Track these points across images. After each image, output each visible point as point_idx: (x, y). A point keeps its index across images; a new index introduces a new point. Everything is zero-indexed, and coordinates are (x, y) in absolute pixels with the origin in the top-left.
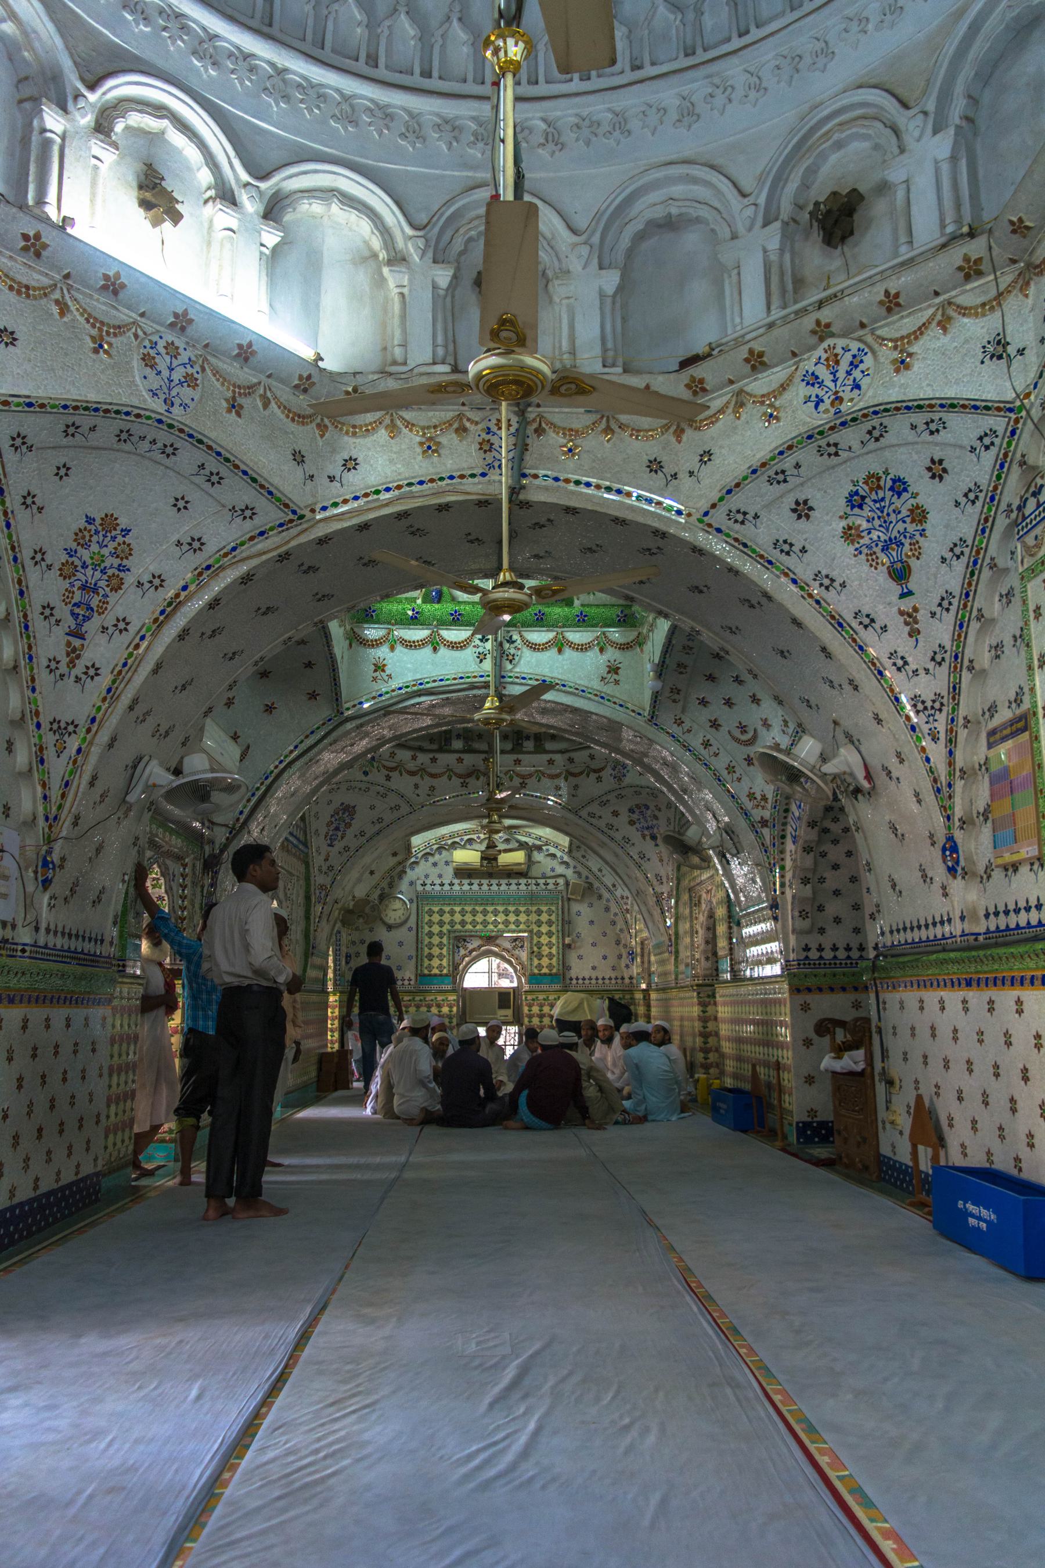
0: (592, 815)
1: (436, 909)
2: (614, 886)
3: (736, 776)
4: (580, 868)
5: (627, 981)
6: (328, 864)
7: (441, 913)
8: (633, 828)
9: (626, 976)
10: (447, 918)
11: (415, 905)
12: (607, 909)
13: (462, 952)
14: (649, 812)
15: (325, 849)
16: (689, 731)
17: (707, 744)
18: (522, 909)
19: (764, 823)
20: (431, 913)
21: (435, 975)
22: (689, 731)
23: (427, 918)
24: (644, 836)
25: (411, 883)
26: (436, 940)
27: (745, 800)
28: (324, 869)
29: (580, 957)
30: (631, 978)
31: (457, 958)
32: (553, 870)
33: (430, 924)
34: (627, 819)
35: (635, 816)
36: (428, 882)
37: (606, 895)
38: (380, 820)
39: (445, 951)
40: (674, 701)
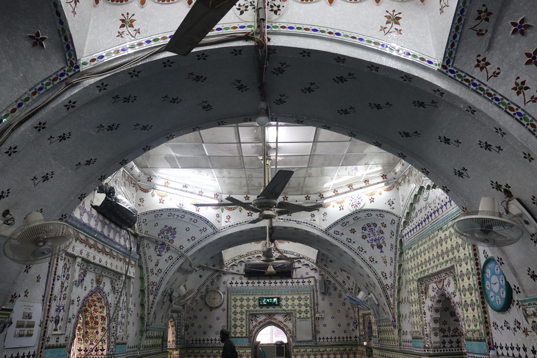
0: (337, 233)
1: (238, 298)
2: (344, 282)
4: (323, 273)
5: (353, 339)
6: (158, 268)
7: (242, 300)
8: (366, 241)
9: (353, 336)
10: (245, 303)
11: (226, 295)
12: (340, 296)
13: (254, 323)
14: (377, 229)
15: (155, 258)
18: (290, 297)
20: (235, 300)
21: (238, 337)
23: (233, 303)
24: (372, 246)
25: (224, 283)
26: (239, 316)
28: (155, 271)
29: (325, 325)
30: (356, 337)
31: (251, 327)
32: (307, 274)
33: (235, 306)
34: (361, 235)
35: (366, 233)
36: (234, 282)
37: (339, 288)
38: (193, 238)
39: (244, 323)
40: (480, 33)
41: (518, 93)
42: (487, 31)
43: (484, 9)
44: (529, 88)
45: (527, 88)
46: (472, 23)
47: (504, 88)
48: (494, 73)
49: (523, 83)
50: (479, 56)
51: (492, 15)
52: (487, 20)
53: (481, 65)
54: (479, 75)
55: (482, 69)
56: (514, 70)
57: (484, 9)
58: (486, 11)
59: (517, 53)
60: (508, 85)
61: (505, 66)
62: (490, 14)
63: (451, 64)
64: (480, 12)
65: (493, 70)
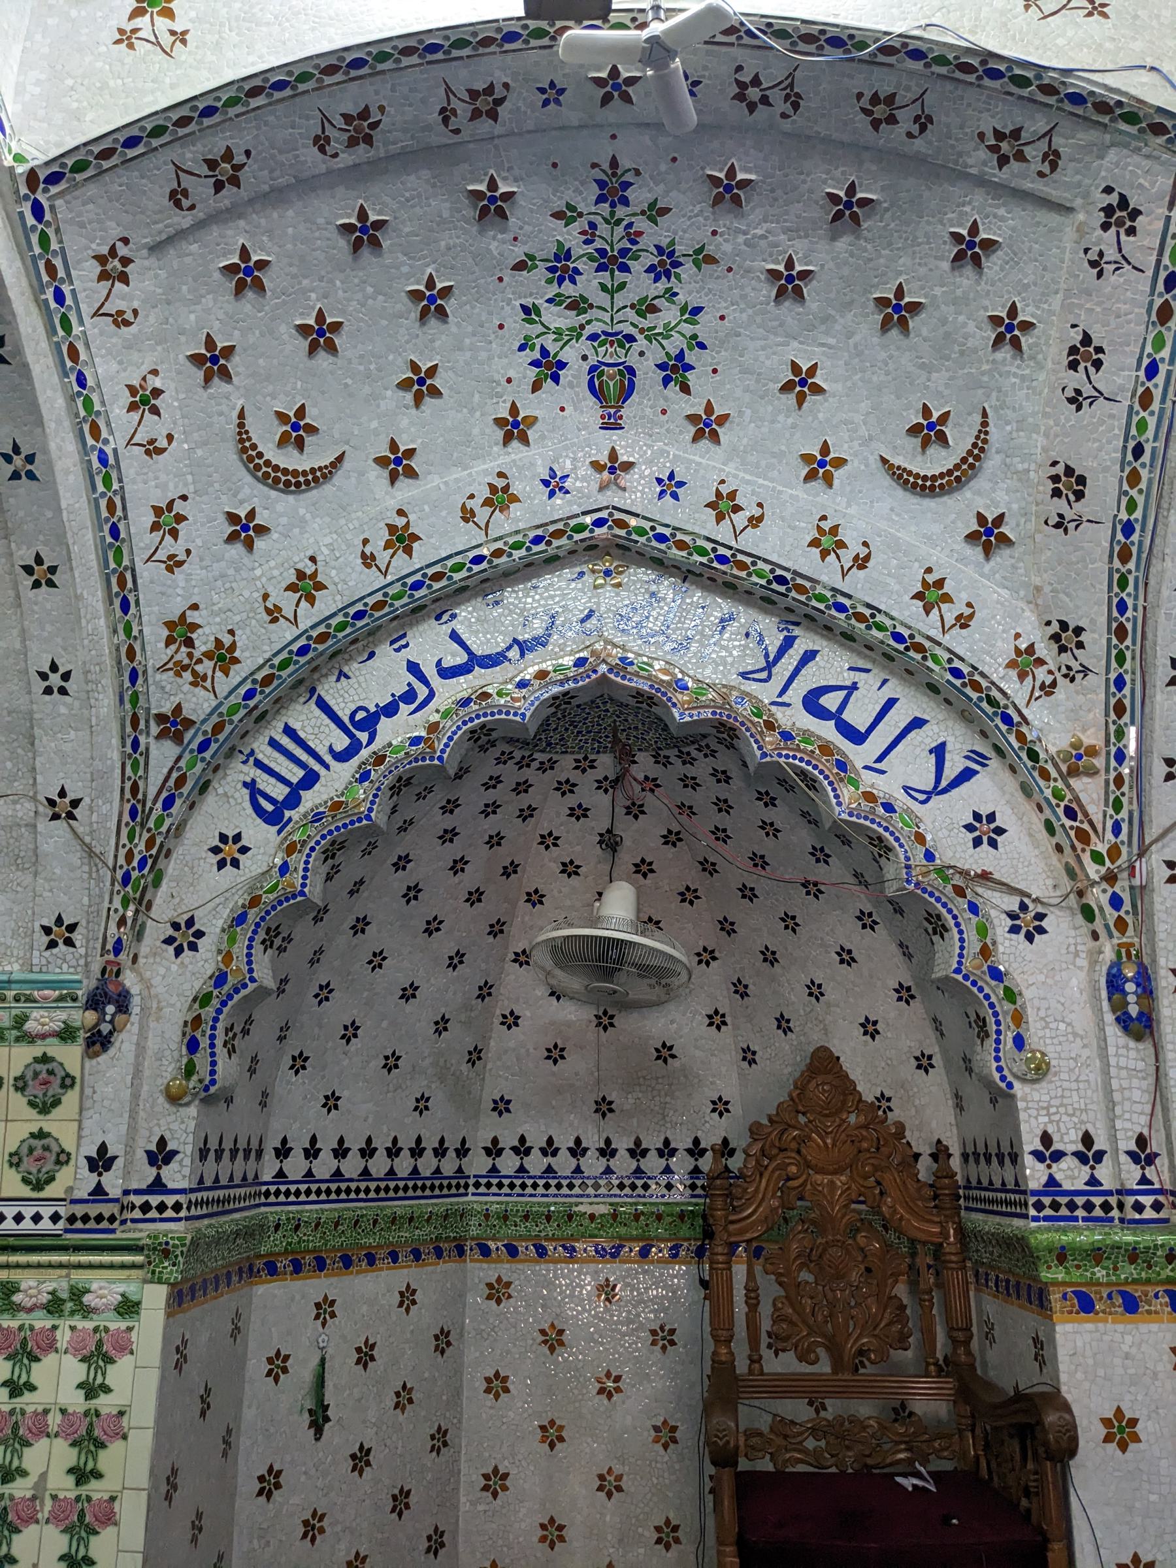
3: (170, 546)
16: (120, 320)
17: (144, 400)
19: (174, 725)
22: (120, 320)
27: (154, 634)
41: (133, 407)
42: (192, 207)
43: (239, 158)
44: (159, 415)
45: (155, 411)
46: (191, 156)
47: (112, 369)
48: (120, 313)
49: (157, 392)
50: (125, 241)
51: (235, 189)
52: (219, 186)
53: (109, 267)
54: (84, 281)
55: (104, 276)
56: (159, 348)
57: (239, 158)
58: (237, 168)
59: (192, 317)
60: (125, 370)
61: (152, 319)
62: (235, 181)
63: (54, 190)
64: (228, 155)
65: (121, 305)
